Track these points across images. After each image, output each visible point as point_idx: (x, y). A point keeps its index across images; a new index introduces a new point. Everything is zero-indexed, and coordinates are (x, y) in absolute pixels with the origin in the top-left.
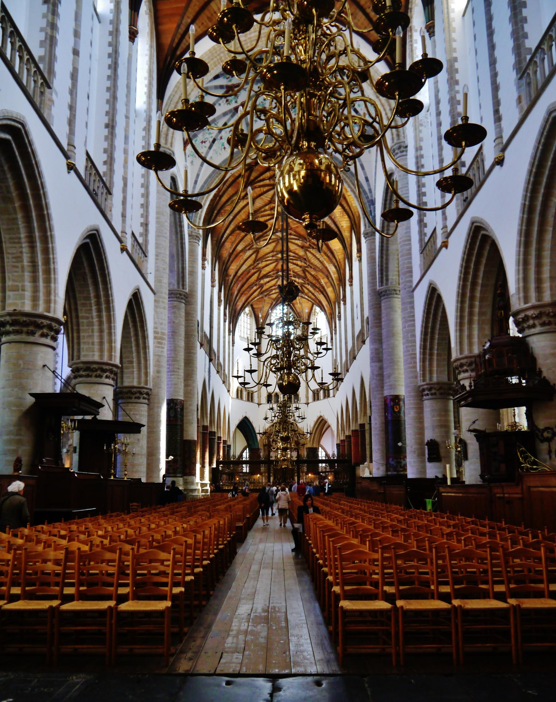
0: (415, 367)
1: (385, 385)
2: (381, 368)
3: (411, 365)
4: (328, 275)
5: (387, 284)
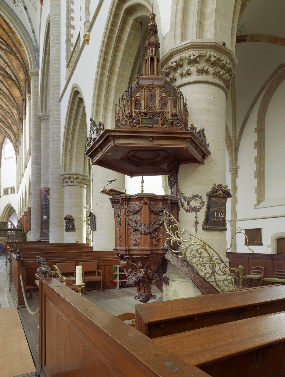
0: (59, 161)
1: (42, 180)
2: (39, 169)
3: (55, 159)
4: (12, 116)
5: (45, 112)
